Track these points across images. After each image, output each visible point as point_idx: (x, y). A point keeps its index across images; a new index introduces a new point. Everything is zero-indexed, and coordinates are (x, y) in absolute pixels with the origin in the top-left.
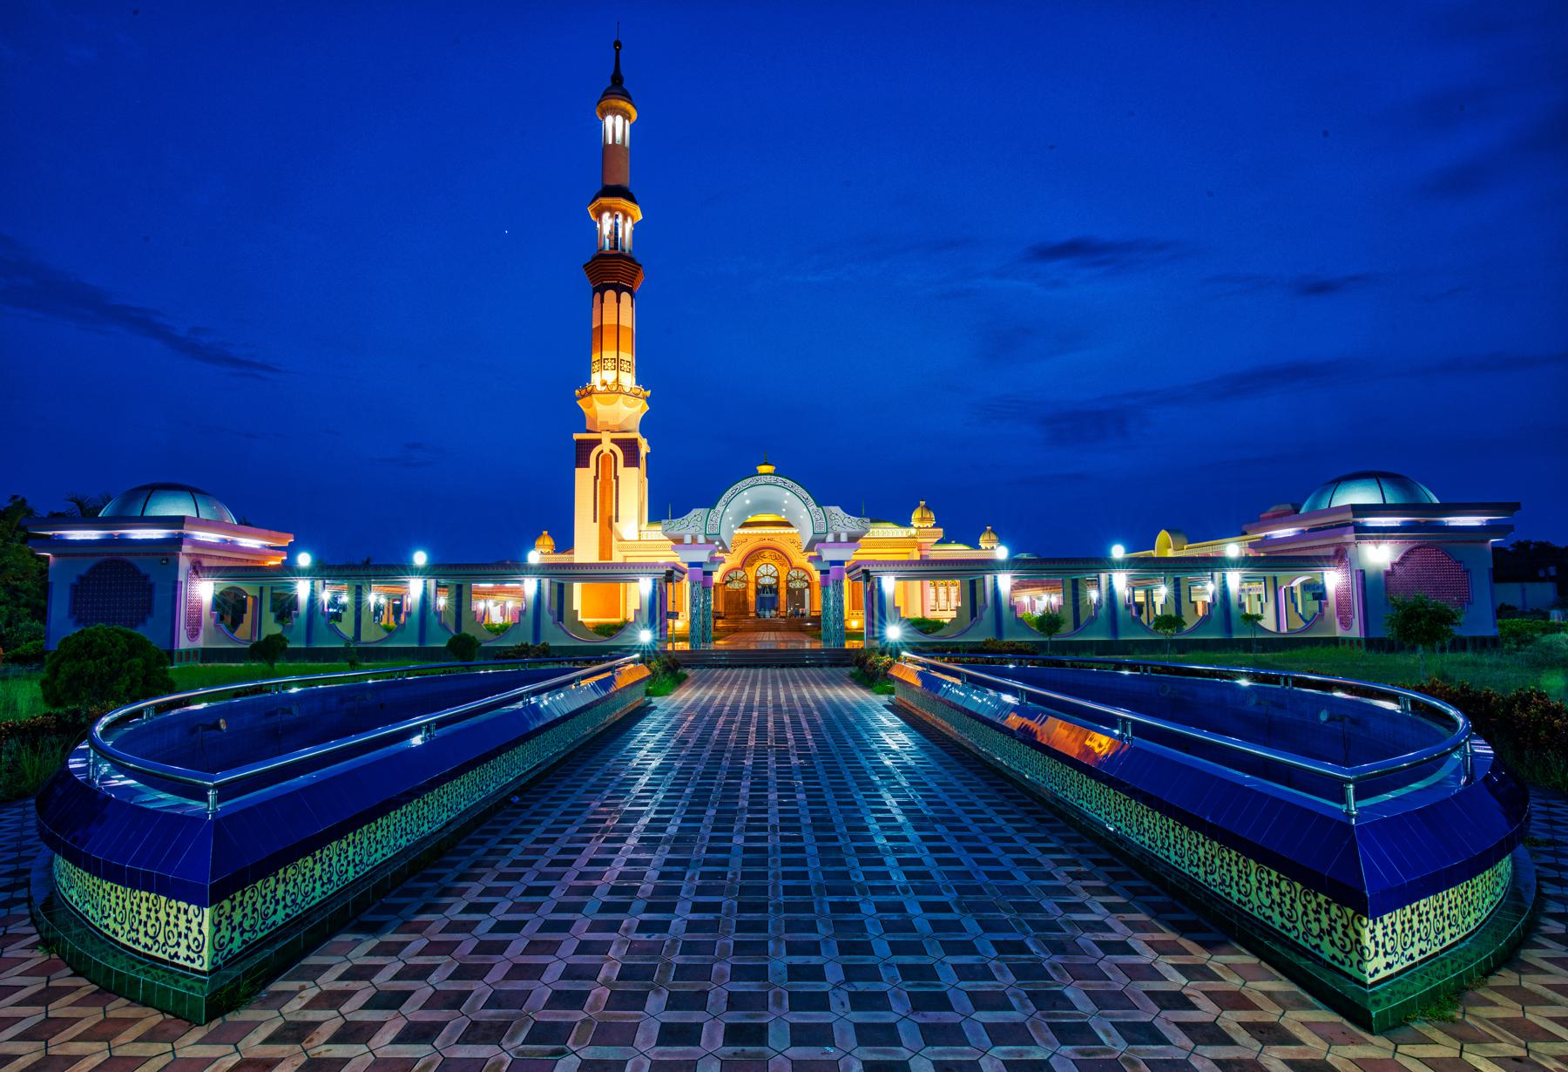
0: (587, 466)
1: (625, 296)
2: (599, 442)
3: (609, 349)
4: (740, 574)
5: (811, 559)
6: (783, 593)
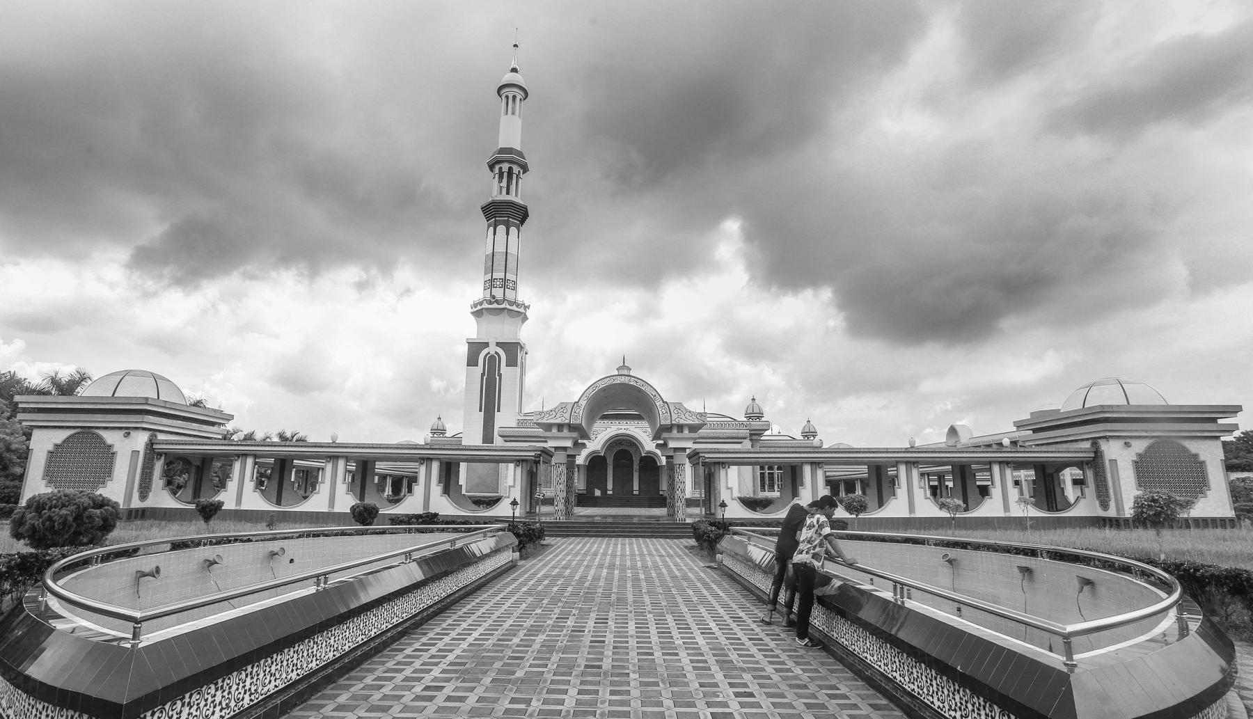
1: (513, 230)
2: (486, 345)
5: (658, 446)
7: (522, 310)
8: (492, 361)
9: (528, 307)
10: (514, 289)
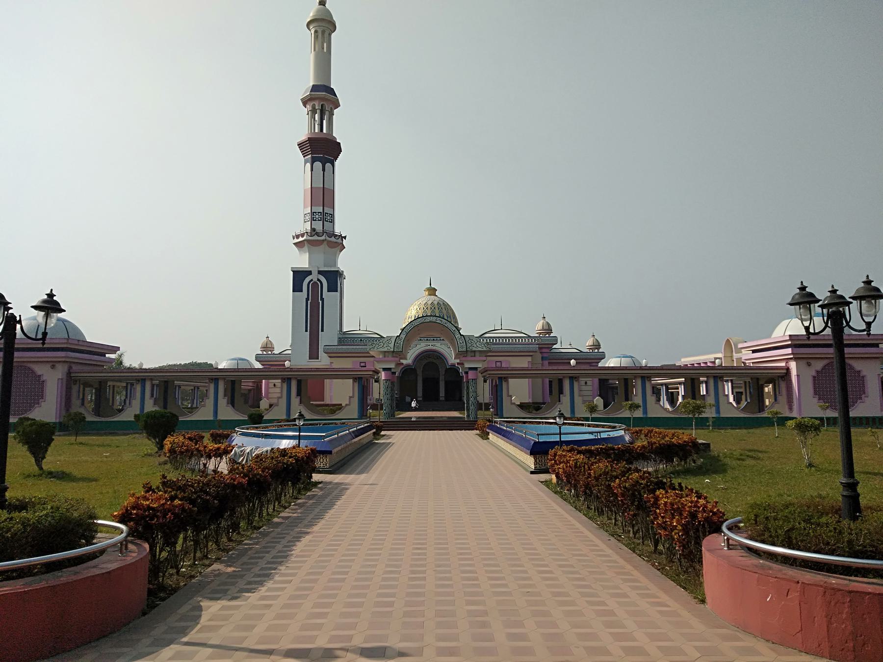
2: (309, 273)
7: (339, 241)
8: (315, 287)
10: (332, 221)
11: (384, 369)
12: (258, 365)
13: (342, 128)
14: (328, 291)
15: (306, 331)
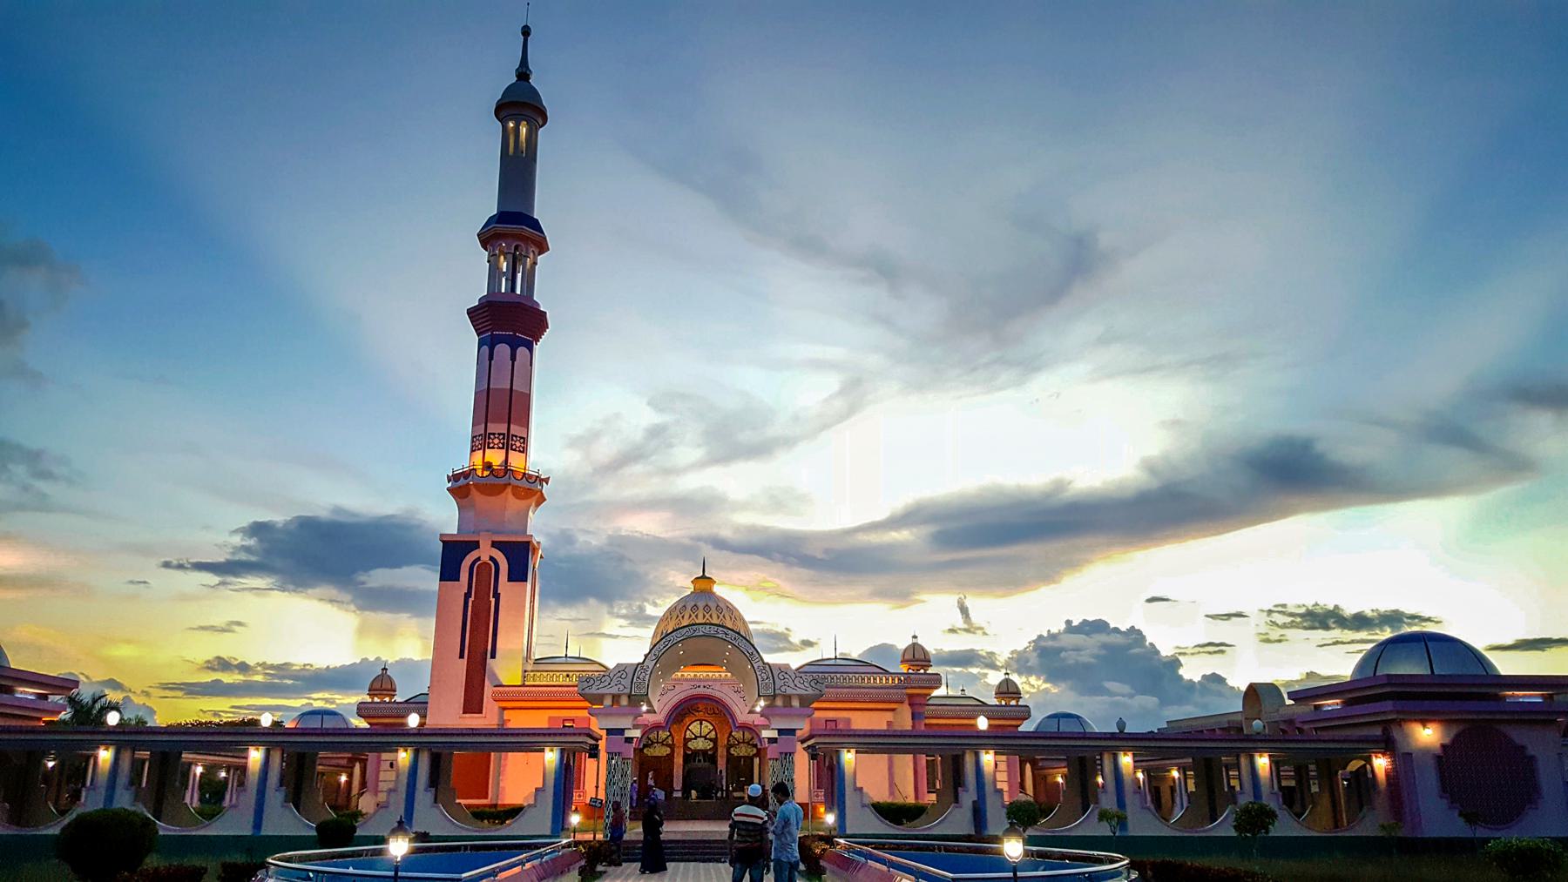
0: (458, 579)
1: (522, 351)
3: (498, 421)
4: (663, 735)
6: (721, 764)
9: (547, 481)
10: (524, 450)
11: (610, 732)
12: (361, 724)
13: (551, 284)
14: (510, 579)
15: (462, 656)
